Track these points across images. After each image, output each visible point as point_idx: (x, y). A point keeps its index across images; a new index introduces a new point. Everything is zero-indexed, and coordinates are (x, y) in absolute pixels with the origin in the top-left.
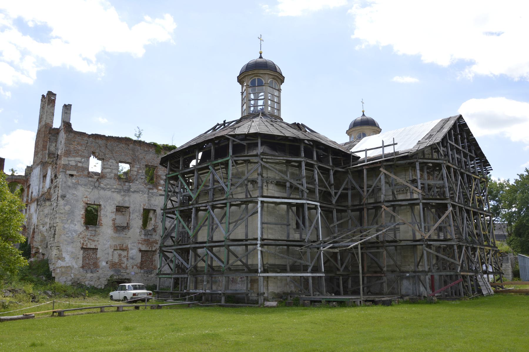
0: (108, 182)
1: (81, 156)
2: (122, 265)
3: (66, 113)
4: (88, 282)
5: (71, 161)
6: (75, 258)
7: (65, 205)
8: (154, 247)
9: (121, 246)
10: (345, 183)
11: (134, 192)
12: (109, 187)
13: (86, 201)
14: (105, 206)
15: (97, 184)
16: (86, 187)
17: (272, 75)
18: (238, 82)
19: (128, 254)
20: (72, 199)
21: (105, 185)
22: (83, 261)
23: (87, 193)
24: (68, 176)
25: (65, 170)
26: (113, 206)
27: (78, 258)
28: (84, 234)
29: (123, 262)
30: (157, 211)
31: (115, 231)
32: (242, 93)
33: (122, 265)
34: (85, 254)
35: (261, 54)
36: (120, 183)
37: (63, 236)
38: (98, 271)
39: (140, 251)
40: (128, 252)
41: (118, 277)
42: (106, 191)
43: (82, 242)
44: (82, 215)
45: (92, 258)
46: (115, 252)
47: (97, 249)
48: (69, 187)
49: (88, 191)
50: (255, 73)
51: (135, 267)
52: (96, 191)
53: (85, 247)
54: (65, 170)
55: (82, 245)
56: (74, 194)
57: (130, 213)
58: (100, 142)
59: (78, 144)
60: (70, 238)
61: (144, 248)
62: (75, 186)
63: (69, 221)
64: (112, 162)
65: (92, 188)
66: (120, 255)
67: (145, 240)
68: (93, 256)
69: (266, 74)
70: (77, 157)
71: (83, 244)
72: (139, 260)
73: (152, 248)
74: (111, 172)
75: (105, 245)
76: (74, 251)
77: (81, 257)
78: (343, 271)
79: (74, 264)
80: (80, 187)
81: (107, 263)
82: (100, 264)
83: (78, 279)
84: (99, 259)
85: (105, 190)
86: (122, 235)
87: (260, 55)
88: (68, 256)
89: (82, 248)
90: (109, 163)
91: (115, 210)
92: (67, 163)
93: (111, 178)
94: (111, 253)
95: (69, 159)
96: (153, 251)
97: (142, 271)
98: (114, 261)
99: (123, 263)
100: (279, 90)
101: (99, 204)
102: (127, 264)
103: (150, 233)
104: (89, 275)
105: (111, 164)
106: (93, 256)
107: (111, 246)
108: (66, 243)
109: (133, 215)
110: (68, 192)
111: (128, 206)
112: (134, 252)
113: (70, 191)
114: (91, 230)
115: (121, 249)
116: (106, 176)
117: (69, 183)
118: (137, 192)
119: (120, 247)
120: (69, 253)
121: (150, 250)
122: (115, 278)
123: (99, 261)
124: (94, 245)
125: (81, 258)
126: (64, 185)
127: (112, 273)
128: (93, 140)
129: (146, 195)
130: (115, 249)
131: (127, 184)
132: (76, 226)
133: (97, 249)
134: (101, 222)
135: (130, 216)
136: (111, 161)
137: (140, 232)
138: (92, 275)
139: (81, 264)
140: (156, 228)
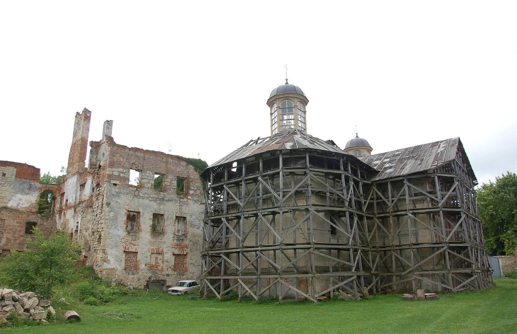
0: (146, 191)
1: (123, 167)
2: (158, 267)
3: (108, 128)
4: (130, 283)
5: (114, 171)
6: (118, 260)
7: (110, 212)
8: (186, 251)
9: (158, 250)
10: (371, 194)
11: (168, 200)
12: (146, 196)
13: (128, 209)
14: (143, 213)
15: (137, 193)
16: (127, 196)
17: (300, 99)
18: (267, 104)
19: (163, 257)
20: (116, 206)
21: (144, 194)
22: (125, 264)
23: (128, 201)
24: (112, 185)
25: (109, 180)
26: (151, 213)
27: (121, 261)
28: (126, 238)
29: (159, 265)
30: (187, 218)
31: (152, 236)
32: (271, 114)
33: (158, 267)
34: (127, 257)
35: (287, 80)
36: (156, 192)
37: (108, 240)
38: (138, 273)
39: (174, 254)
40: (163, 255)
41: (155, 278)
42: (144, 200)
43: (124, 246)
44: (124, 221)
45: (132, 260)
46: (153, 256)
47: (137, 252)
48: (113, 195)
49: (129, 200)
50: (286, 97)
51: (169, 269)
52: (136, 199)
53: (127, 251)
54: (109, 180)
55: (124, 249)
56: (117, 202)
57: (164, 220)
58: (139, 154)
59: (120, 156)
60: (114, 242)
61: (177, 252)
62: (118, 194)
63: (114, 226)
64: (149, 174)
65: (132, 196)
66: (156, 258)
67: (177, 245)
69: (295, 97)
70: (119, 168)
71: (125, 248)
72: (172, 263)
73: (183, 252)
74: (148, 183)
75: (143, 249)
76: (118, 254)
77: (124, 260)
78: (375, 271)
79: (118, 266)
80: (122, 195)
81: (146, 265)
82: (140, 266)
83: (122, 280)
84: (139, 262)
85: (143, 199)
86: (159, 239)
87: (286, 81)
88: (113, 259)
89: (125, 252)
90: (147, 174)
91: (152, 217)
92: (111, 173)
93: (148, 188)
94: (149, 257)
95: (113, 169)
96: (184, 255)
97: (176, 273)
98: (151, 263)
99: (160, 266)
100: (305, 112)
101: (138, 211)
102: (163, 266)
103: (181, 239)
104: (131, 276)
105: (149, 175)
106: (133, 259)
107: (149, 250)
108: (111, 247)
109: (167, 222)
110: (112, 200)
111: (163, 214)
112: (169, 256)
113: (114, 199)
114: (132, 235)
115: (157, 253)
116: (144, 185)
117: (113, 192)
118: (171, 201)
119: (157, 250)
120: (113, 256)
121: (182, 254)
122: (153, 279)
123: (139, 263)
124: (134, 249)
125: (124, 262)
126: (108, 193)
127: (150, 275)
128: (133, 153)
129: (178, 204)
130: (153, 252)
131: (161, 193)
132: (120, 232)
133: (137, 252)
134: (140, 228)
135: (164, 223)
136: (148, 172)
137: (173, 237)
138: (133, 276)
139: (124, 267)
140: (187, 233)
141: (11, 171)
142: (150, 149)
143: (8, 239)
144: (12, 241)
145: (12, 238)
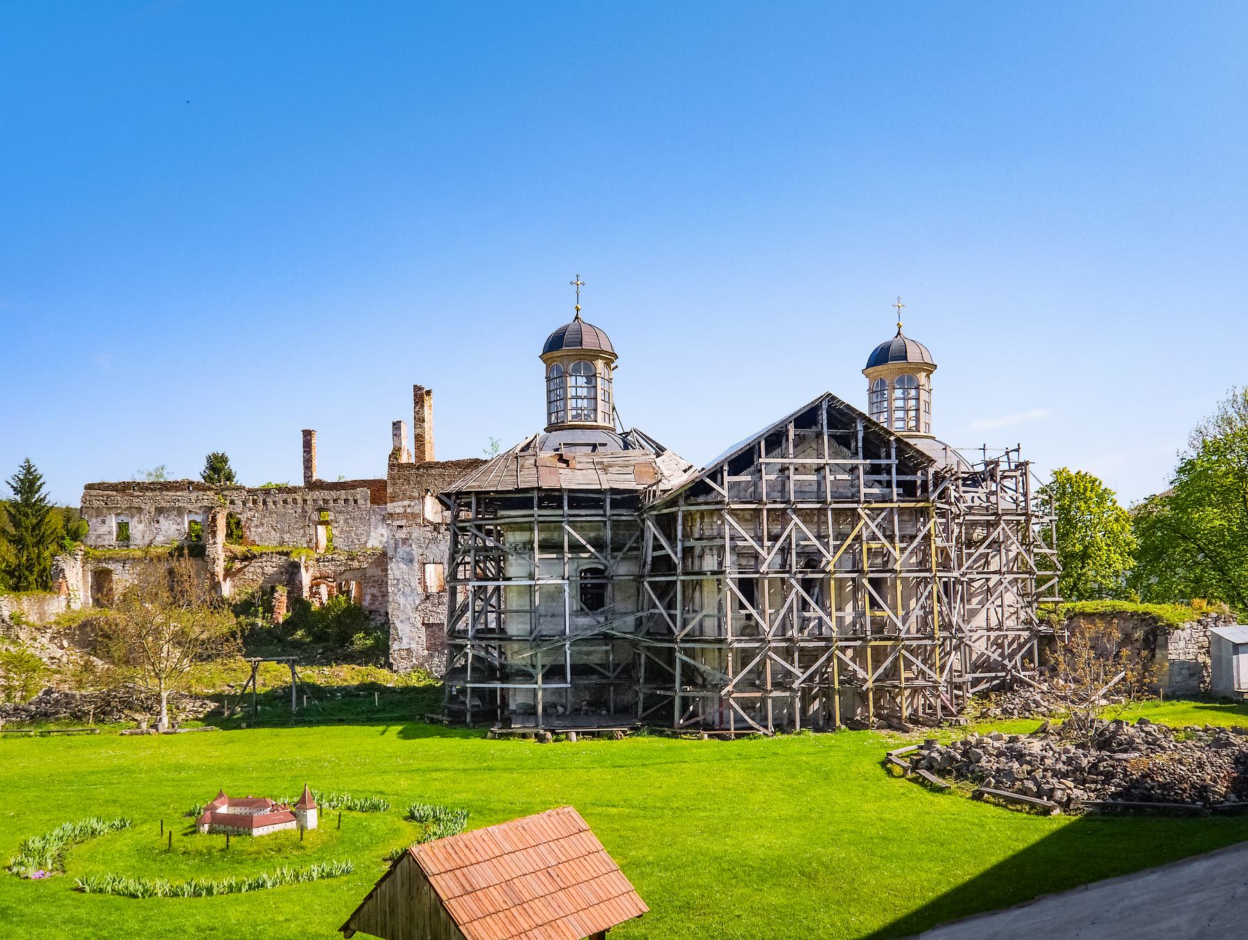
141: (362, 494)
143: (373, 596)
144: (380, 598)
145: (379, 594)
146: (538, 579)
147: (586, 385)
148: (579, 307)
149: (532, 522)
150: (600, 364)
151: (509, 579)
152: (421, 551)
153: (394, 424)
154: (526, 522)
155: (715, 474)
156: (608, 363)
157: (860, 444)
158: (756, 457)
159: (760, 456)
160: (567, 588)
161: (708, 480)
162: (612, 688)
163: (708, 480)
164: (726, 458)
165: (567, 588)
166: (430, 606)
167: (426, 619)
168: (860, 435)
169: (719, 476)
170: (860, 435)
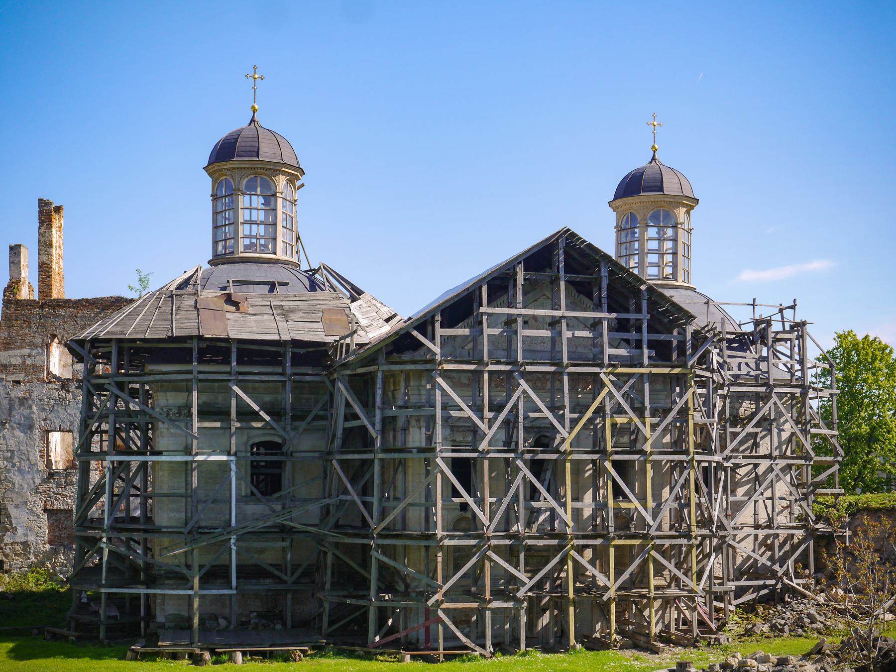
17: (248, 168)
34: (53, 519)
45: (64, 526)
53: (50, 508)
68: (65, 522)
69: (234, 168)
106: (65, 522)
142: (90, 296)
146: (197, 454)
147: (263, 207)
148: (257, 107)
149: (191, 380)
150: (281, 182)
151: (159, 453)
152: (43, 415)
153: (11, 248)
154: (182, 380)
155: (424, 324)
156: (292, 179)
157: (604, 294)
158: (475, 305)
159: (481, 305)
160: (233, 466)
161: (415, 333)
162: (289, 596)
163: (415, 333)
164: (439, 306)
165: (233, 466)
166: (54, 486)
167: (49, 503)
168: (605, 282)
169: (430, 328)
170: (605, 282)
